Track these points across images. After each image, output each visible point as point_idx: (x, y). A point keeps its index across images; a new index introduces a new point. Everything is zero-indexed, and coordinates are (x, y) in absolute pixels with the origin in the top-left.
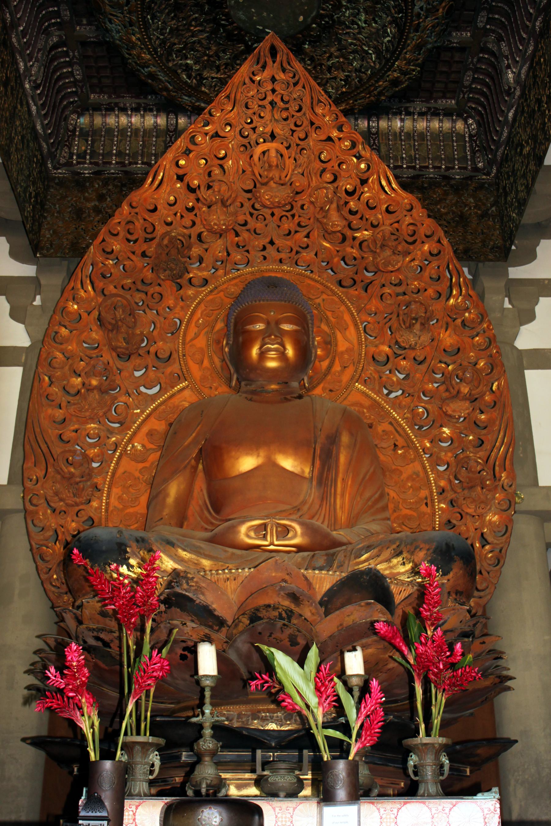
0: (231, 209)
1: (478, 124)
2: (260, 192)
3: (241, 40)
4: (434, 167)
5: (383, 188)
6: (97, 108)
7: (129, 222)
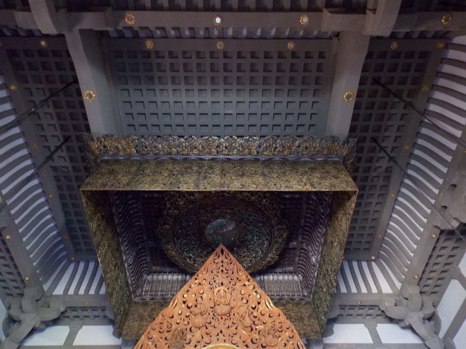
0: (205, 316)
1: (303, 277)
2: (216, 309)
3: (210, 246)
4: (287, 295)
5: (267, 306)
6: (155, 272)
7: (161, 323)
